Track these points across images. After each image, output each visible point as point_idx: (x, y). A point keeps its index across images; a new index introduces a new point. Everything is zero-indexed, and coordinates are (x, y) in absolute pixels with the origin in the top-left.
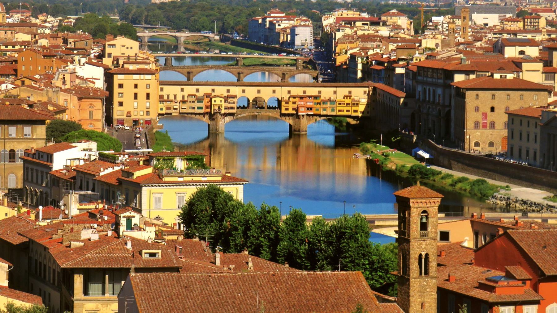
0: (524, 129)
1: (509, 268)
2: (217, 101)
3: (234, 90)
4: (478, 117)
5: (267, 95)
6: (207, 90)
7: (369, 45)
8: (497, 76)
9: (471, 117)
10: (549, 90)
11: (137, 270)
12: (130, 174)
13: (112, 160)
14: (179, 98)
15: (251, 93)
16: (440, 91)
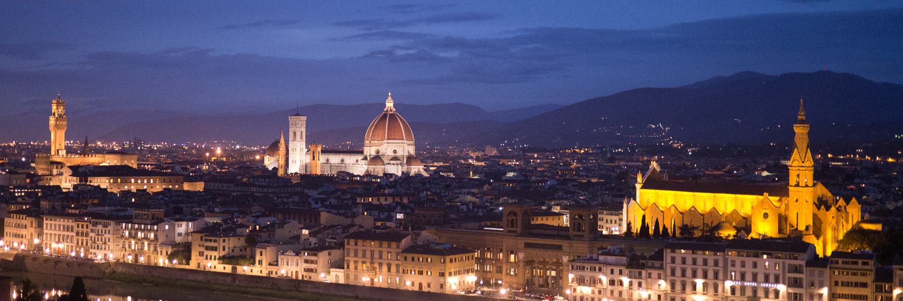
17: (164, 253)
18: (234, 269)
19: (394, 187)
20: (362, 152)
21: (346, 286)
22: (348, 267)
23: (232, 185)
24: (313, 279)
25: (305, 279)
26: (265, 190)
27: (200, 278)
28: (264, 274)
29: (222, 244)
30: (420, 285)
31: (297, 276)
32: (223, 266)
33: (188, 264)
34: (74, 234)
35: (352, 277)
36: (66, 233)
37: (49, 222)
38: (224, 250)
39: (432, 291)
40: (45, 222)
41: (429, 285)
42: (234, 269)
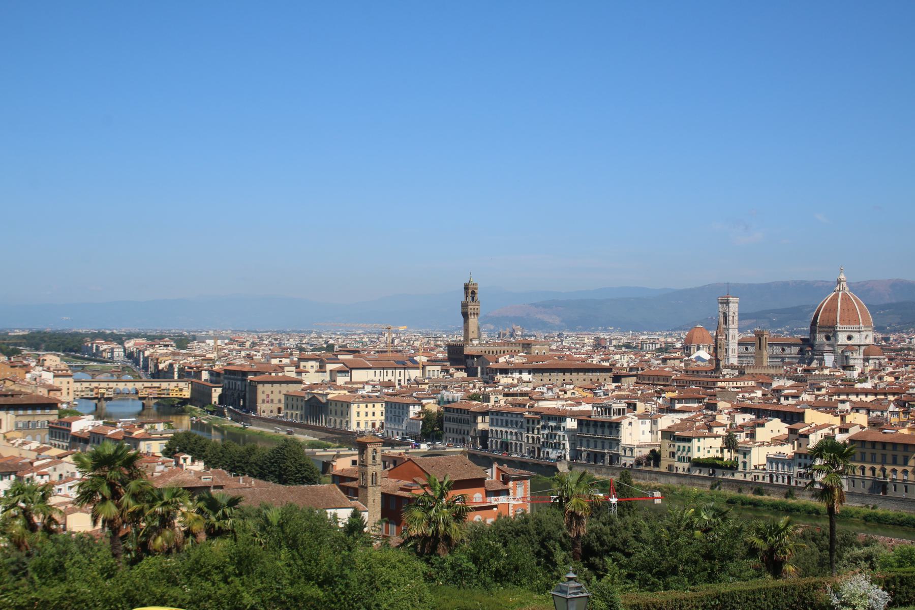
0: (295, 402)
1: (415, 479)
2: (102, 391)
3: (111, 385)
4: (264, 397)
5: (130, 386)
6: (96, 384)
7: (176, 358)
8: (273, 374)
9: (260, 397)
10: (300, 382)
11: (215, 487)
12: (131, 433)
13: (114, 425)
14: (80, 389)
15: (121, 386)
16: (239, 383)
19: (865, 381)
28: (749, 478)
31: (789, 482)
38: (699, 450)
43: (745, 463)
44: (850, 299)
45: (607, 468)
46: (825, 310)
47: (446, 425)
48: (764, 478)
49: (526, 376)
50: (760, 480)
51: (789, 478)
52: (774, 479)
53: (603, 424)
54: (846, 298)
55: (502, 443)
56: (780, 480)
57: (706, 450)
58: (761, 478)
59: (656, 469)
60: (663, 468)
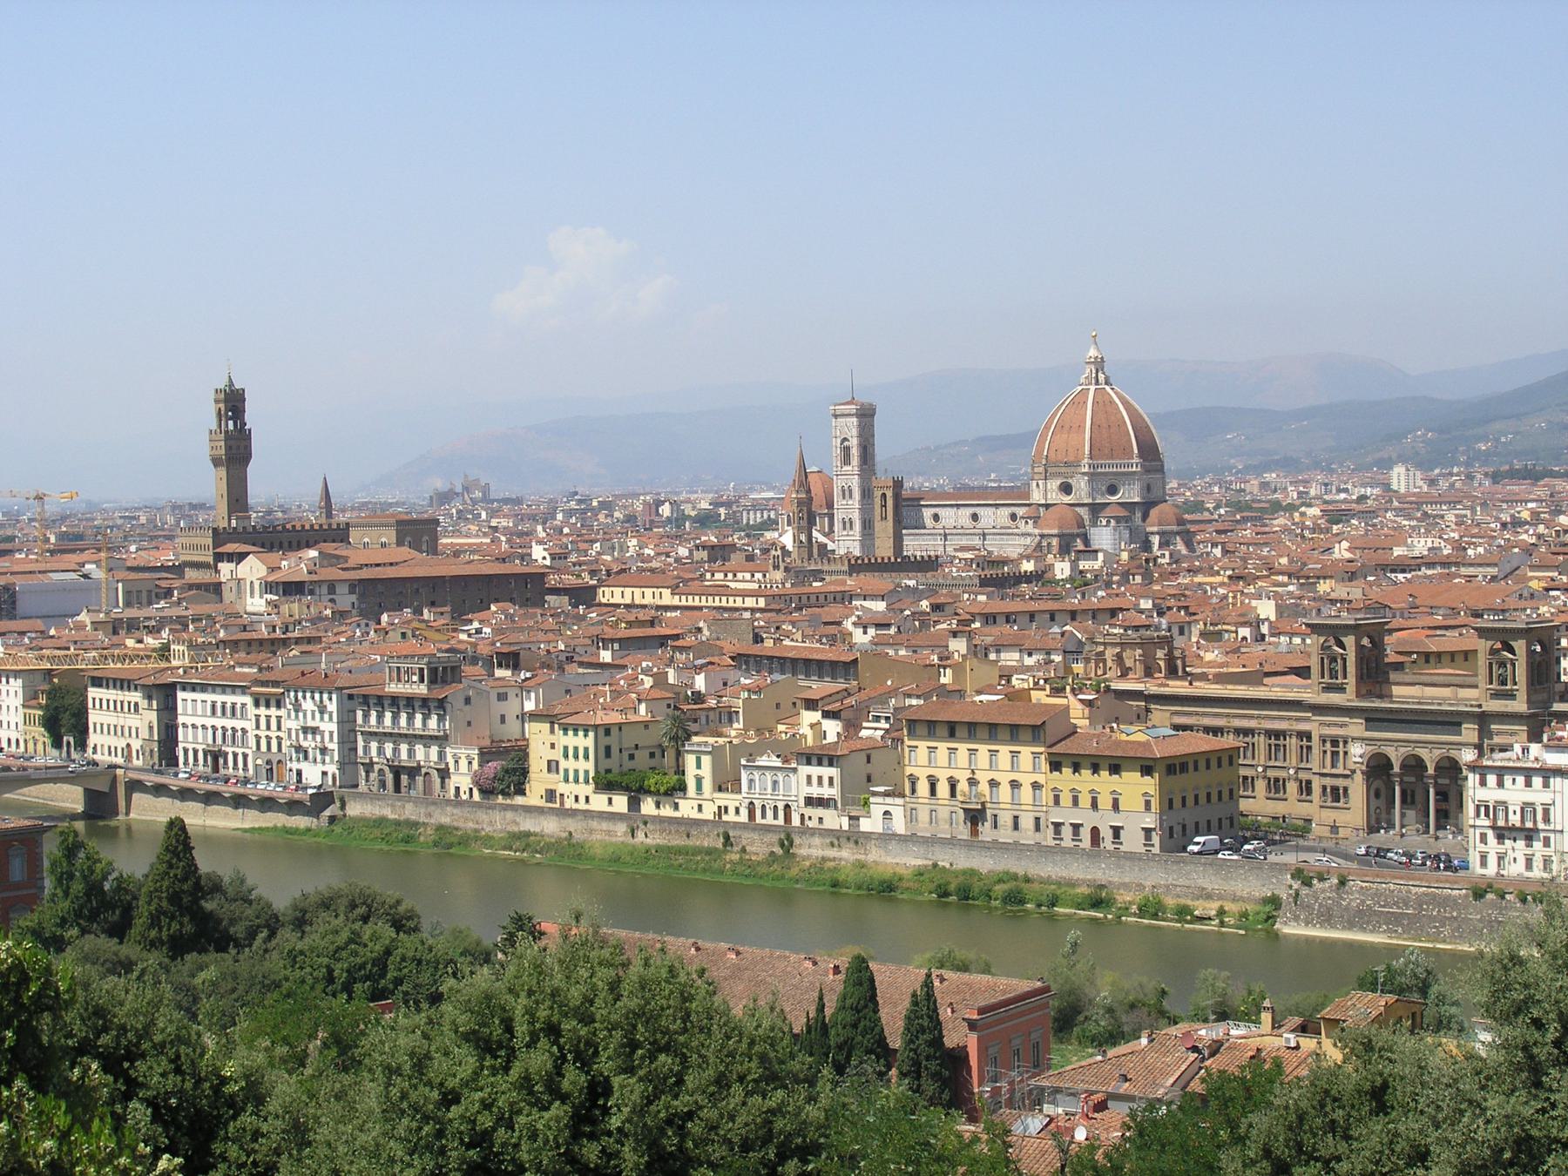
17: (463, 763)
18: (634, 804)
20: (1027, 495)
21: (909, 839)
22: (913, 791)
23: (666, 592)
24: (827, 825)
25: (811, 824)
26: (750, 602)
27: (550, 827)
28: (708, 813)
29: (605, 741)
30: (1095, 832)
31: (788, 818)
32: (605, 798)
33: (522, 792)
34: (249, 725)
35: (923, 815)
36: (229, 723)
37: (189, 695)
39: (1122, 848)
40: (181, 695)
41: (1117, 831)
42: (634, 804)
43: (699, 780)
44: (1112, 402)
45: (416, 801)
46: (1061, 426)
47: (94, 717)
48: (737, 811)
49: (346, 600)
50: (730, 817)
51: (787, 807)
52: (758, 813)
53: (410, 703)
54: (1103, 403)
55: (205, 753)
56: (770, 813)
57: (626, 755)
58: (732, 810)
59: (519, 800)
60: (534, 795)
